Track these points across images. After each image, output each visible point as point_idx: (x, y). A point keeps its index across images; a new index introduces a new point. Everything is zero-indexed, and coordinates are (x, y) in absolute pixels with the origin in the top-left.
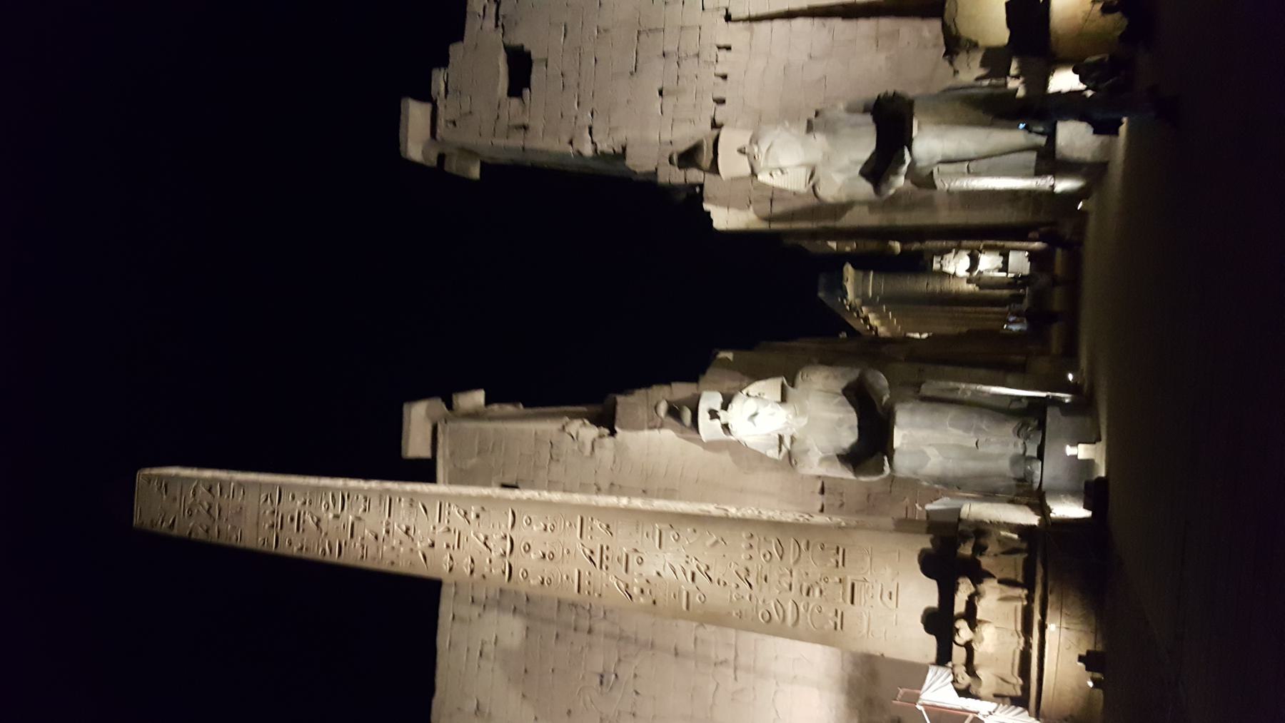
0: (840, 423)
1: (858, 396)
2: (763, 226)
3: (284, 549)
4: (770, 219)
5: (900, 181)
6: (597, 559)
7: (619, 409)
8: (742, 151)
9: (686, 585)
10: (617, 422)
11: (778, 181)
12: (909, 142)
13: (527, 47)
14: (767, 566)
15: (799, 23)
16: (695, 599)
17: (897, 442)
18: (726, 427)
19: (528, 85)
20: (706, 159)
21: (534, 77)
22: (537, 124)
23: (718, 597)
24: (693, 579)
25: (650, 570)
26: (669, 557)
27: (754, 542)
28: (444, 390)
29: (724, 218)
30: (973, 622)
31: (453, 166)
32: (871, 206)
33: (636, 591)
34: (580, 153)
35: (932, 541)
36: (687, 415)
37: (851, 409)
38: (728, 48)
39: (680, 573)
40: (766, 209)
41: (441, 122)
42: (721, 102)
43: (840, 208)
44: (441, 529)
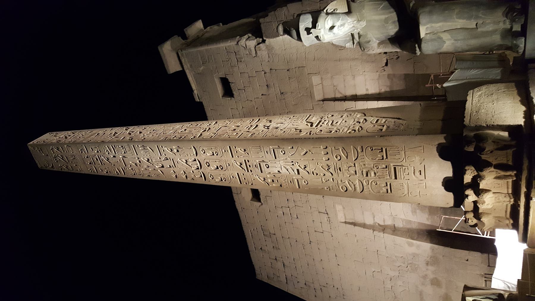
0: (386, 21)
6: (244, 166)
7: (262, 26)
9: (296, 177)
10: (264, 35)
14: (339, 163)
17: (422, 35)
18: (317, 37)
23: (315, 181)
24: (299, 173)
27: (329, 150)
30: (478, 192)
33: (269, 181)
35: (445, 138)
36: (294, 33)
37: (392, 10)
39: (290, 170)
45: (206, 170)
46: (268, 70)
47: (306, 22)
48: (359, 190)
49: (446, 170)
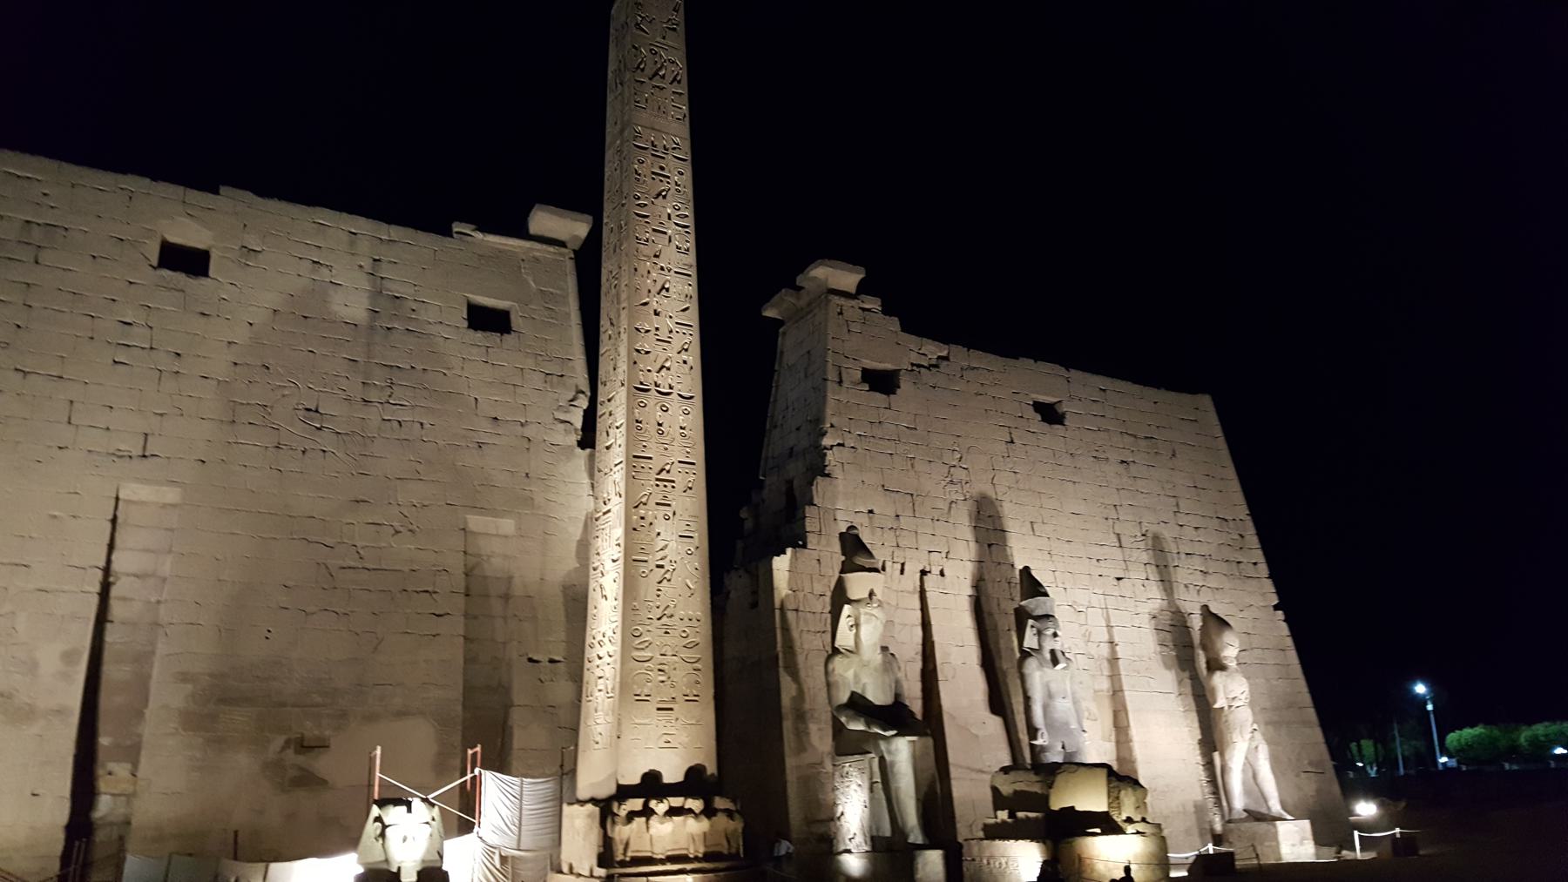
2: (777, 604)
4: (782, 609)
6: (663, 476)
8: (871, 594)
15: (919, 632)
16: (643, 568)
19: (871, 389)
21: (878, 395)
26: (673, 545)
27: (694, 623)
34: (824, 434)
38: (902, 572)
39: (662, 554)
40: (790, 605)
41: (842, 301)
45: (652, 399)
46: (528, 432)
48: (636, 654)
49: (672, 773)
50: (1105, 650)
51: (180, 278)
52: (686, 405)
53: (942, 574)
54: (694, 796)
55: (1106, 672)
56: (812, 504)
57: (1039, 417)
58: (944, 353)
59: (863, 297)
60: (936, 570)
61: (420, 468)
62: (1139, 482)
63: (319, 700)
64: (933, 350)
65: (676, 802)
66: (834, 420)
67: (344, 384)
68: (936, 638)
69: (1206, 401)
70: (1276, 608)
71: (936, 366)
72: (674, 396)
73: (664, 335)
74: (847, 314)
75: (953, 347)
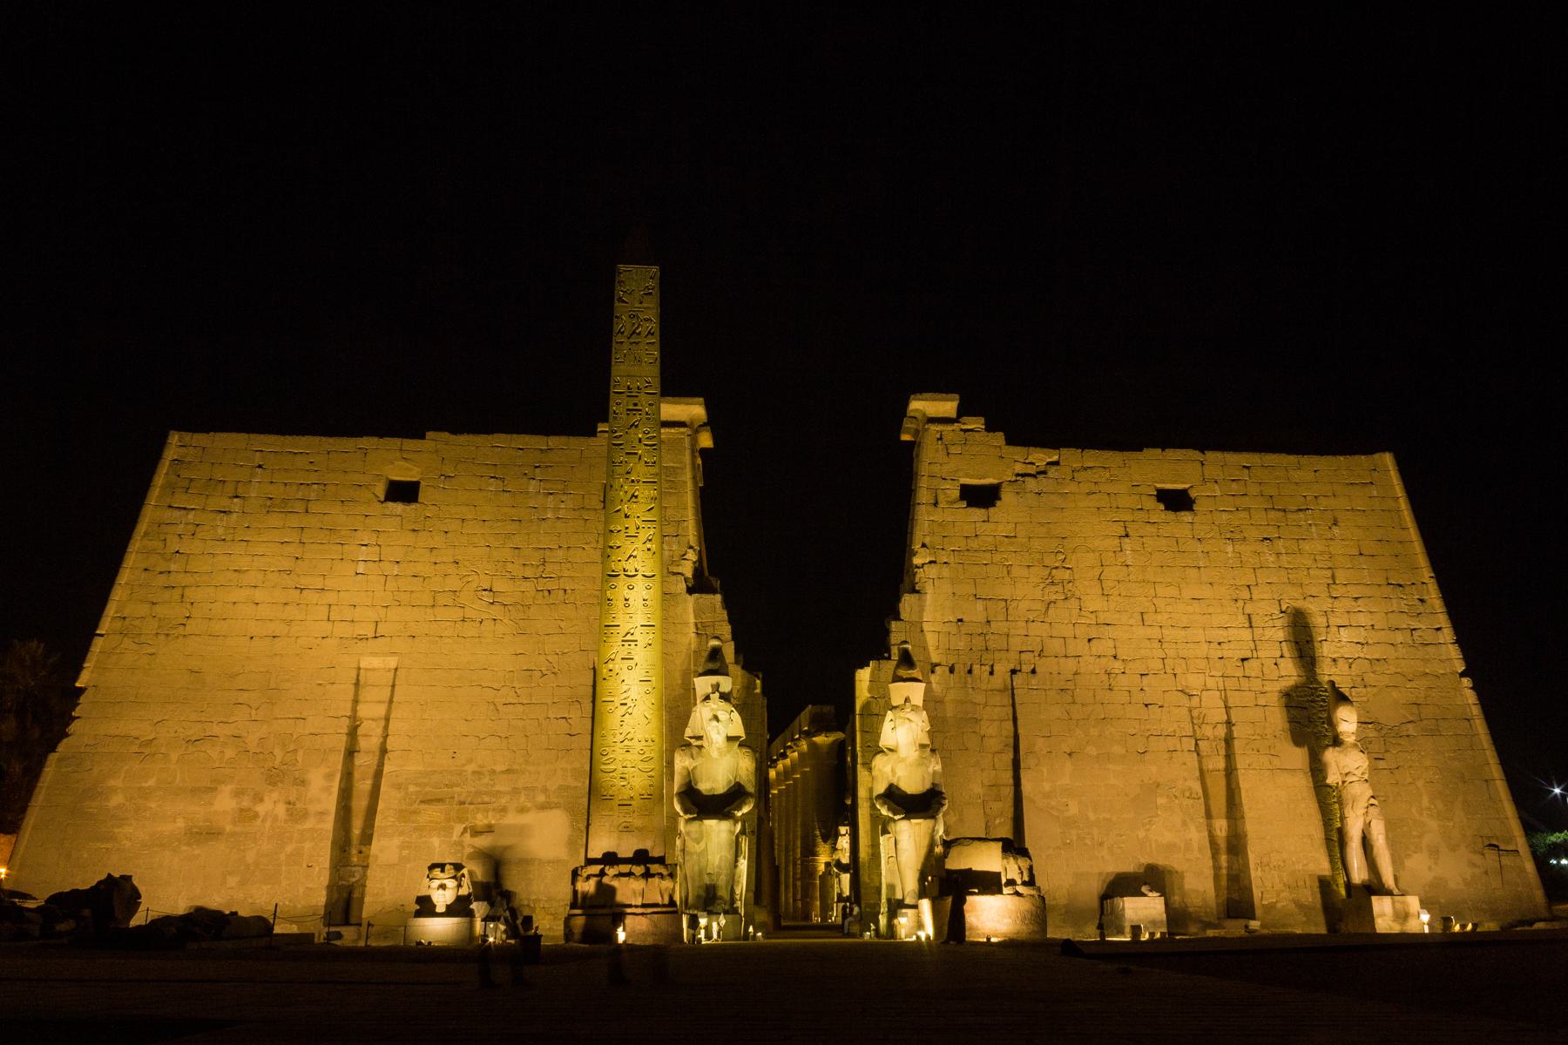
1: (736, 794)
3: (614, 399)
5: (884, 811)
6: (629, 637)
8: (907, 700)
11: (887, 726)
12: (907, 818)
13: (998, 503)
18: (707, 698)
19: (970, 505)
20: (903, 673)
22: (937, 516)
25: (625, 674)
28: (714, 422)
29: (863, 676)
31: (907, 424)
32: (871, 790)
38: (991, 673)
41: (940, 427)
42: (952, 670)
43: (870, 770)
44: (638, 522)
45: (621, 582)
47: (726, 684)
50: (1221, 731)
51: (398, 507)
52: (648, 582)
53: (1033, 671)
54: (638, 864)
55: (1223, 752)
56: (897, 618)
57: (1162, 507)
58: (1055, 458)
59: (965, 419)
60: (1027, 668)
61: (563, 624)
62: (1284, 557)
63: (486, 799)
64: (1040, 457)
65: (624, 868)
66: (927, 540)
67: (510, 567)
68: (1020, 731)
69: (1387, 459)
70: (1462, 675)
71: (1044, 472)
72: (639, 577)
73: (632, 532)
74: (948, 437)
75: (1064, 451)
